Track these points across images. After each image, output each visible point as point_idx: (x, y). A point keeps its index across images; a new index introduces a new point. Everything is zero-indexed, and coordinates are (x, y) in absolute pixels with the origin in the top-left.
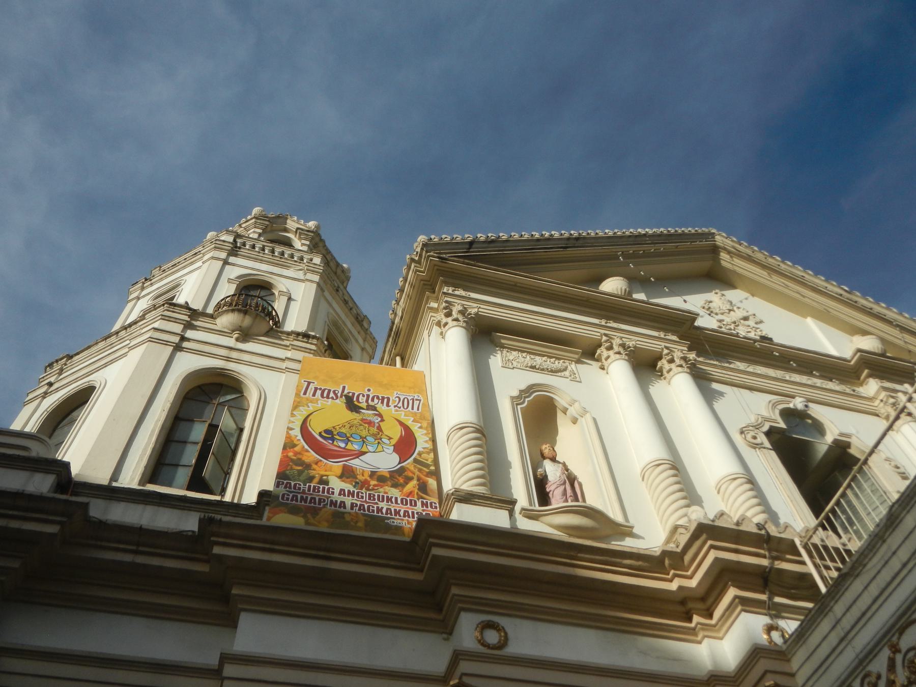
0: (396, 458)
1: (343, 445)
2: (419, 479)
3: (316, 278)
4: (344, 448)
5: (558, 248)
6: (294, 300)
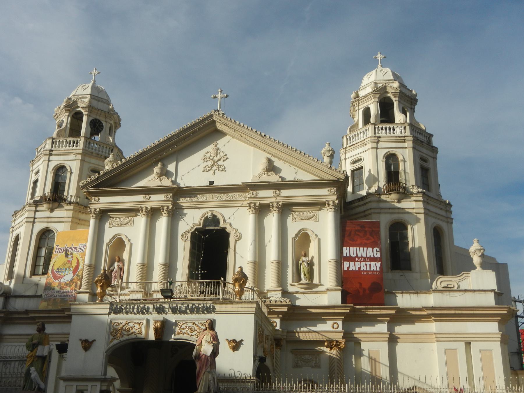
0: (72, 274)
1: (60, 274)
2: (76, 283)
3: (79, 157)
4: (60, 275)
5: (134, 162)
6: (73, 173)
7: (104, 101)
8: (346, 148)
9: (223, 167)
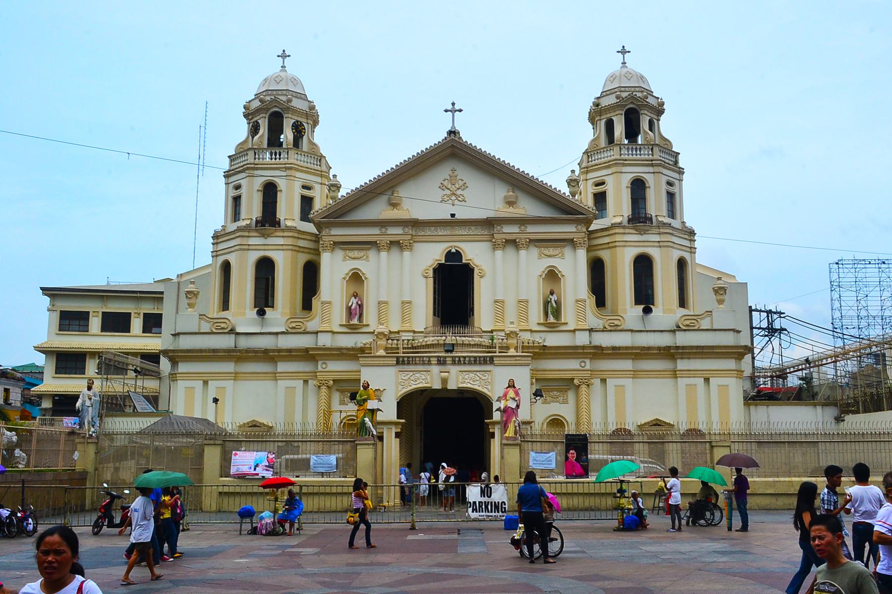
7: (303, 96)
8: (587, 168)
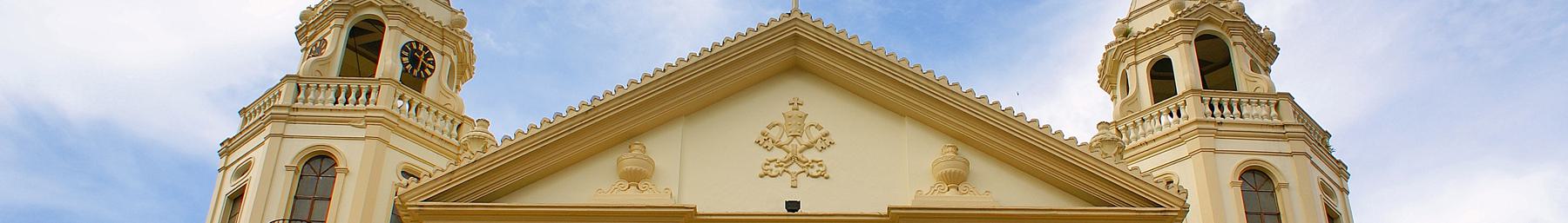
9: (821, 165)
